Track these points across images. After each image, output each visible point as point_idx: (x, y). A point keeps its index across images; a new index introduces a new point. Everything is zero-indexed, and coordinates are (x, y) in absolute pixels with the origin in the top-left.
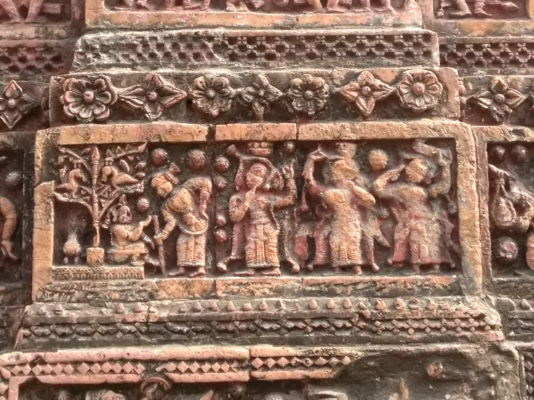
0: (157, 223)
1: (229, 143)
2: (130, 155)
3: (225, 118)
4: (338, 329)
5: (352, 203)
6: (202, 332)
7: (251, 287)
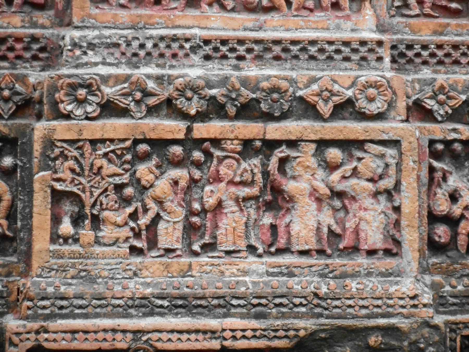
0: (140, 210)
1: (205, 140)
2: (118, 149)
3: (202, 116)
4: (296, 306)
5: (311, 195)
6: (181, 306)
7: (223, 268)
